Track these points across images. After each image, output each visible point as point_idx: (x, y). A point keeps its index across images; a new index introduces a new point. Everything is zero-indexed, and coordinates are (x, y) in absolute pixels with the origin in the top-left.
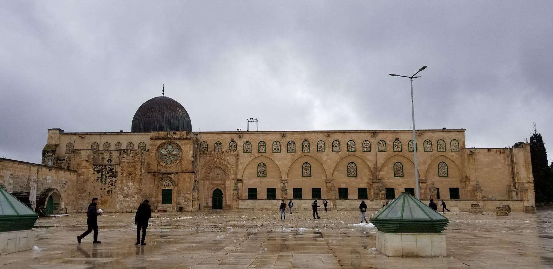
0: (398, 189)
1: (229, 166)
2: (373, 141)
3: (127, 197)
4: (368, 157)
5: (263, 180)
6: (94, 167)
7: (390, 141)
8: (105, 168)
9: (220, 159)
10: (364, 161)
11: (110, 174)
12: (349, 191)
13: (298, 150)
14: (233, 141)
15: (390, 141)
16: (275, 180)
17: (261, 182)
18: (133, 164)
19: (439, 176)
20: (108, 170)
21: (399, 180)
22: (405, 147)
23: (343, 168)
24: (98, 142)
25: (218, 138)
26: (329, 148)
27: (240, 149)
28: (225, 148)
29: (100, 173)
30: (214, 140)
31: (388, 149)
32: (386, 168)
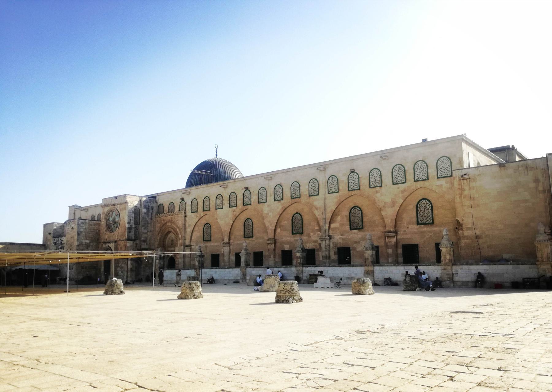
2: (322, 178)
4: (315, 203)
5: (208, 244)
13: (240, 202)
14: (182, 199)
17: (206, 247)
19: (418, 224)
21: (356, 235)
22: (365, 182)
23: (286, 223)
27: (188, 208)
28: (177, 209)
31: (340, 188)
32: (339, 218)
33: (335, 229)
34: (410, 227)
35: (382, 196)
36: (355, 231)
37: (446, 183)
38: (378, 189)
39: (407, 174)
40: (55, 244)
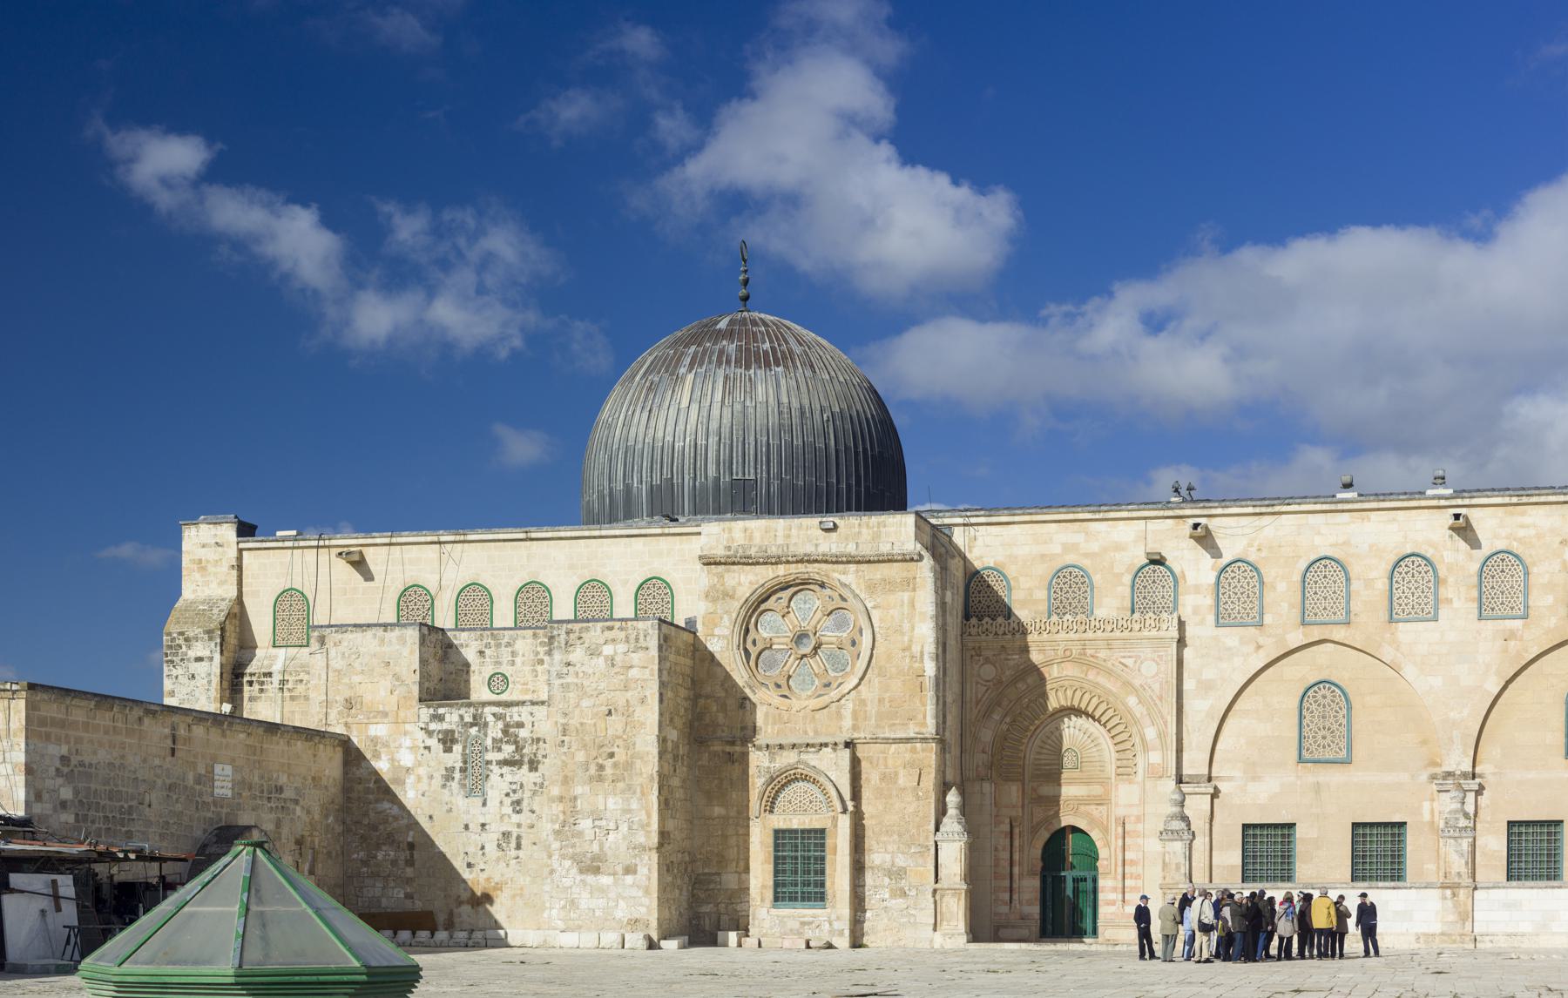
3: (596, 871)
5: (1333, 777)
6: (426, 713)
8: (477, 721)
9: (1082, 661)
11: (508, 749)
18: (620, 699)
20: (495, 730)
24: (431, 583)
25: (1068, 548)
27: (1196, 604)
28: (1110, 603)
29: (457, 748)
40: (448, 740)
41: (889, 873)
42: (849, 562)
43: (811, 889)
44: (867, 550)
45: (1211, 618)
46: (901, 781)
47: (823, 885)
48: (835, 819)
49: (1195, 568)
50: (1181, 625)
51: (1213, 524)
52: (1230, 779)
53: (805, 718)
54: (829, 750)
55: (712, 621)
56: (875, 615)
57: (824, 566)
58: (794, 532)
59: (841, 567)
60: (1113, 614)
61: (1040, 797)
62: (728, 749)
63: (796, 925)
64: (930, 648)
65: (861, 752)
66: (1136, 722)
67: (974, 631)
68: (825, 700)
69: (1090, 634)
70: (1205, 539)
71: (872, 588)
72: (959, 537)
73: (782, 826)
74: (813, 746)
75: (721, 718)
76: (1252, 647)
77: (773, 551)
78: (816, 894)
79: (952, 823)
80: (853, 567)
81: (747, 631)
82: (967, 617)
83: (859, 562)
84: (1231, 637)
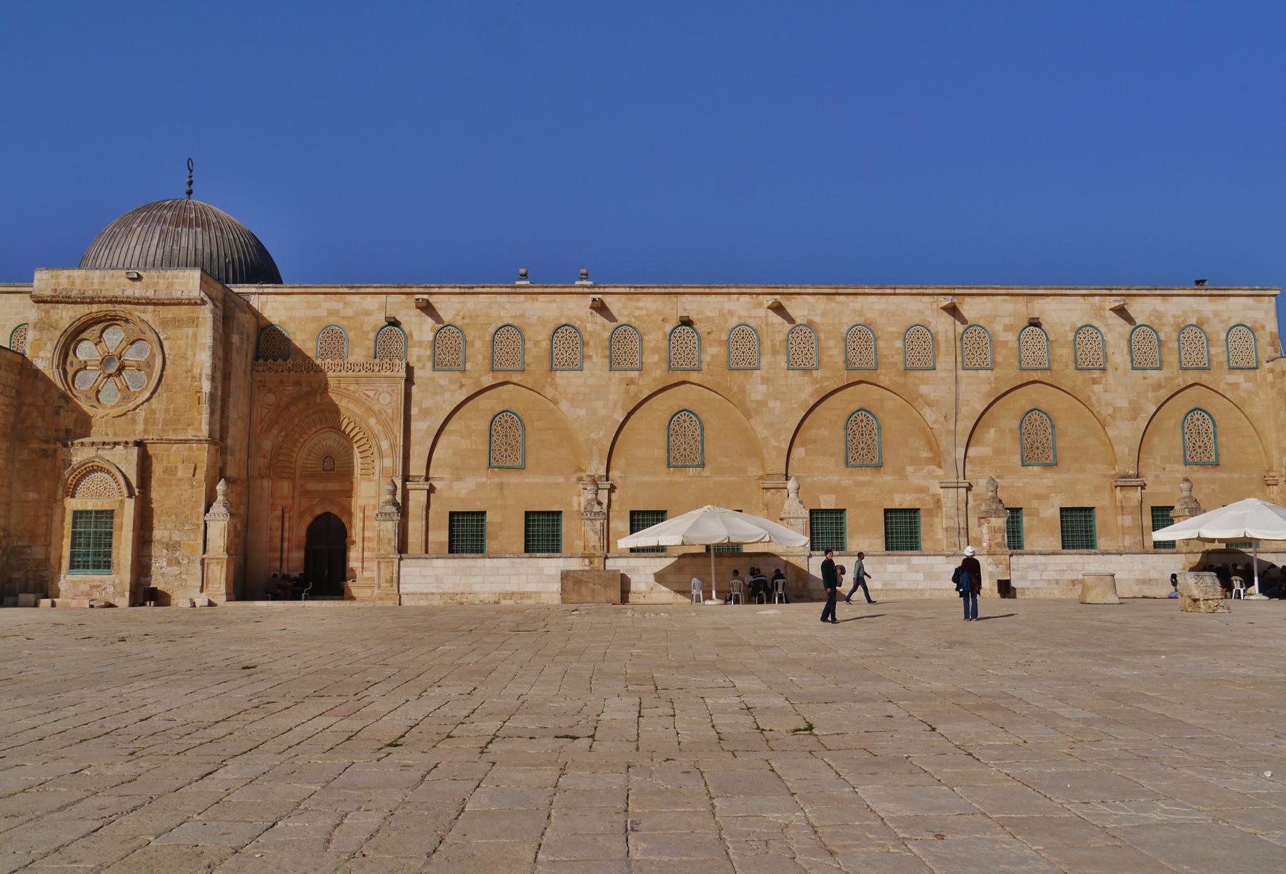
0: (1035, 513)
1: (372, 421)
4: (924, 389)
5: (512, 479)
7: (1008, 328)
10: (912, 399)
12: (849, 518)
15: (1008, 328)
16: (561, 479)
17: (501, 486)
25: (331, 313)
26: (775, 352)
27: (419, 355)
28: (359, 354)
30: (315, 319)
31: (999, 359)
32: (992, 434)
33: (982, 460)
34: (1168, 467)
35: (1105, 391)
36: (1036, 468)
37: (1247, 381)
38: (1096, 374)
39: (1165, 350)
41: (167, 546)
42: (147, 304)
43: (101, 559)
44: (162, 295)
45: (429, 365)
46: (180, 473)
47: (109, 555)
48: (122, 502)
49: (420, 329)
50: (409, 369)
51: (433, 299)
52: (441, 479)
53: (106, 423)
54: (120, 448)
55: (38, 345)
56: (166, 344)
57: (129, 307)
58: (107, 279)
59: (142, 307)
60: (361, 360)
61: (307, 492)
62: (44, 446)
63: (85, 588)
64: (207, 370)
65: (151, 449)
66: (375, 437)
67: (261, 368)
68: (124, 409)
69: (344, 373)
70: (428, 309)
71: (165, 323)
72: (255, 302)
73: (80, 508)
74: (108, 444)
75: (40, 423)
76: (457, 386)
77: (90, 293)
78: (104, 563)
79: (218, 508)
80: (151, 308)
81: (67, 355)
82: (257, 358)
83: (155, 304)
84: (443, 379)
